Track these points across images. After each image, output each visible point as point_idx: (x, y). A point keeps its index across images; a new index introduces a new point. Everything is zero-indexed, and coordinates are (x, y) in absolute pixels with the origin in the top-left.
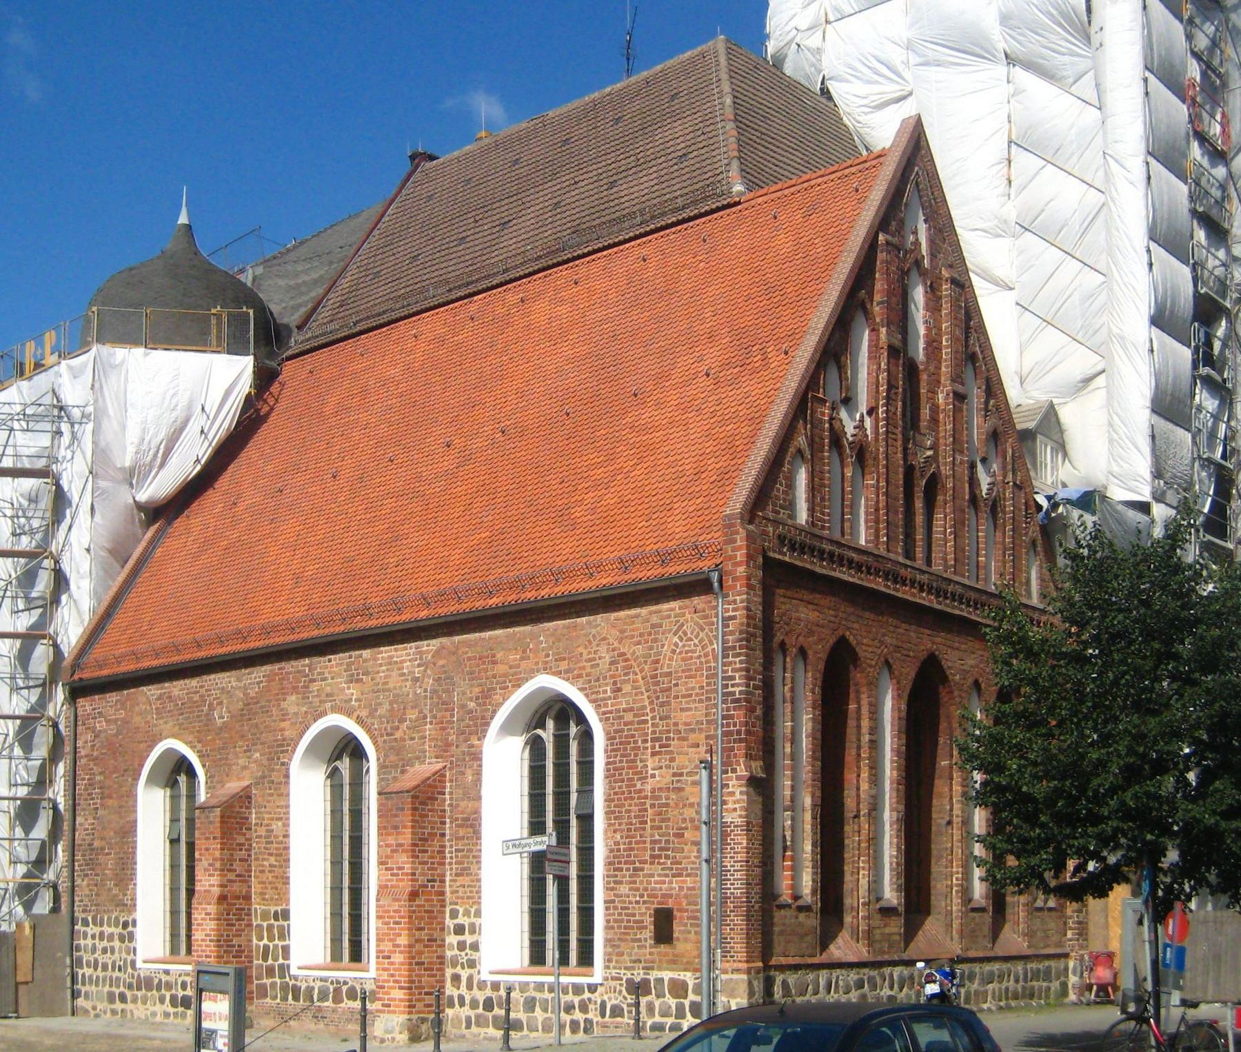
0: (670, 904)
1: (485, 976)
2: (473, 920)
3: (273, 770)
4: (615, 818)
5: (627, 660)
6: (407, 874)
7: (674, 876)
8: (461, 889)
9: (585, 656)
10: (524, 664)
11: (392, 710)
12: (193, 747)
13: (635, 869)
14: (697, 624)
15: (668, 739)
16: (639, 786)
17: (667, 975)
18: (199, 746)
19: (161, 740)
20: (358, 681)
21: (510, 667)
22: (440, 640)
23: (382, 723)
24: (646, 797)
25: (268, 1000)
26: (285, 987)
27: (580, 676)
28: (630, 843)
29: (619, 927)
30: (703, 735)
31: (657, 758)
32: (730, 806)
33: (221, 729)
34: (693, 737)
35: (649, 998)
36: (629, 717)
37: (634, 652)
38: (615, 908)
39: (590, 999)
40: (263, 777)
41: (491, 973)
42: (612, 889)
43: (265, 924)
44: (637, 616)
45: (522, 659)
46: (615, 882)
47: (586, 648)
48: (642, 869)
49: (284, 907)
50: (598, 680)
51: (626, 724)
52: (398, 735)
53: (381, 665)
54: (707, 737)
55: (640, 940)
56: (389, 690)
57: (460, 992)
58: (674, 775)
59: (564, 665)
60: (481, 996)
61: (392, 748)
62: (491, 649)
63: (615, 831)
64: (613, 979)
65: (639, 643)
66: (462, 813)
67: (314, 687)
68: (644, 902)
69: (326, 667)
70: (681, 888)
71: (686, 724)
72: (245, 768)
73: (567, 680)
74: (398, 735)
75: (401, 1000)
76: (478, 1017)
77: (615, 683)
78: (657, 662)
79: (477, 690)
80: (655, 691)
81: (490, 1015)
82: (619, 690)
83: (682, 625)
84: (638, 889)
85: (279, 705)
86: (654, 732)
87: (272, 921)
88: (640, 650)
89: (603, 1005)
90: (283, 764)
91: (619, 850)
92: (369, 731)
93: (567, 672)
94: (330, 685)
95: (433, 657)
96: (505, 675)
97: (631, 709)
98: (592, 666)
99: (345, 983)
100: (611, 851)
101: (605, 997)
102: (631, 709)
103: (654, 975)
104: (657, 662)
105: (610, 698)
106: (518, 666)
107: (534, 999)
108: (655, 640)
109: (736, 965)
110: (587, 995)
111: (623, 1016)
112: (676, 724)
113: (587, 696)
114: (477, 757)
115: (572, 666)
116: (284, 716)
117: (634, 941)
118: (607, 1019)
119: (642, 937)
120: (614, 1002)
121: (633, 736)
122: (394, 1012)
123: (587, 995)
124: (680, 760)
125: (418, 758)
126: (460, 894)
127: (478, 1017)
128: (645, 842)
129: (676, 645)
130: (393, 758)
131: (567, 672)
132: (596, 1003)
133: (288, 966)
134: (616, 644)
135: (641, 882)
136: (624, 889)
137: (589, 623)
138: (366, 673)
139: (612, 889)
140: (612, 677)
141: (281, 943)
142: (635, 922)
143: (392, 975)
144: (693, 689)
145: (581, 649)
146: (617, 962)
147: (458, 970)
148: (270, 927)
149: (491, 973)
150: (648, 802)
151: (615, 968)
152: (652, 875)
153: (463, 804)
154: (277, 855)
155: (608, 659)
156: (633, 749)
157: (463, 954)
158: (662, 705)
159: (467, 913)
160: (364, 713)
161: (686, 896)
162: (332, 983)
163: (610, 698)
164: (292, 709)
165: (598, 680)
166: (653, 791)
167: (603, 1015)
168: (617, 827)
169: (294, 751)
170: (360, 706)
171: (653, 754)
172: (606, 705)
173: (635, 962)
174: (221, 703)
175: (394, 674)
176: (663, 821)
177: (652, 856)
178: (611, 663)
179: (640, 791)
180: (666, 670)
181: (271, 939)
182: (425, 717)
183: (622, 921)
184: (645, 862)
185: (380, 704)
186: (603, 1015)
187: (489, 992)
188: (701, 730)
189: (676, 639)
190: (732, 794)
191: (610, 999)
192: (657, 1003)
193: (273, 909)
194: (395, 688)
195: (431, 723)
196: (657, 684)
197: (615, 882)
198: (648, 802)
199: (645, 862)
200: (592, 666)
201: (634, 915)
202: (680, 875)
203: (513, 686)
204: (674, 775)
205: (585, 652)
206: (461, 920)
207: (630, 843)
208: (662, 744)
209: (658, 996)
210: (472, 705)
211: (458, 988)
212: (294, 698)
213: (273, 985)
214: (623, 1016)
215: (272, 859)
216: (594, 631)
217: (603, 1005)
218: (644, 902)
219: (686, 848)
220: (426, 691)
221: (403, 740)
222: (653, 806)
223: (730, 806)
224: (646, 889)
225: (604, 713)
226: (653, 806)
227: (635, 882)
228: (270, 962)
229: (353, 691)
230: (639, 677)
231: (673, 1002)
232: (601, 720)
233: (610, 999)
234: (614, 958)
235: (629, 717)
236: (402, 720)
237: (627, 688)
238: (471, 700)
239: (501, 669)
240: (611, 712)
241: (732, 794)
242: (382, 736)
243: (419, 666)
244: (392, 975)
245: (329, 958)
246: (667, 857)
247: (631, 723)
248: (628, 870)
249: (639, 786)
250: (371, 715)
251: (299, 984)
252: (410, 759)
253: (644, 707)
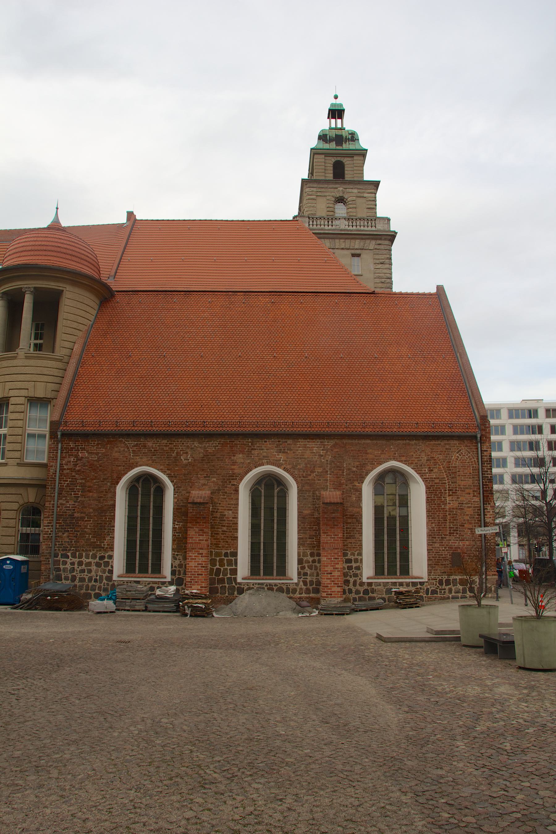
0: (459, 551)
1: (365, 580)
2: (356, 557)
3: (226, 487)
4: (432, 518)
5: (435, 460)
6: (340, 538)
7: (460, 540)
8: (349, 544)
9: (414, 456)
10: (383, 456)
11: (306, 467)
12: (164, 472)
13: (442, 538)
14: (467, 450)
15: (456, 490)
16: (443, 507)
17: (458, 577)
18: (169, 472)
19: (137, 467)
20: (284, 452)
21: (375, 456)
22: (336, 440)
23: (300, 472)
24: (446, 511)
25: (219, 594)
26: (232, 589)
27: (412, 463)
28: (439, 528)
29: (435, 560)
30: (472, 490)
31: (451, 497)
32: (488, 516)
33: (187, 465)
34: (467, 491)
35: (450, 586)
36: (437, 481)
37: (438, 457)
38: (433, 552)
39: (421, 588)
40: (219, 490)
41: (368, 578)
42: (431, 545)
43: (218, 559)
44: (440, 444)
45: (382, 454)
46: (433, 542)
47: (414, 453)
48: (446, 538)
49: (232, 550)
50: (421, 466)
51: (435, 483)
52: (310, 478)
53: (299, 447)
54: (473, 491)
55: (445, 564)
56: (305, 458)
57: (349, 587)
58: (459, 503)
59: (404, 458)
60: (362, 589)
61: (307, 483)
62: (364, 448)
63: (432, 523)
64: (432, 579)
65: (441, 454)
66: (350, 512)
67: (256, 452)
68: (447, 550)
69: (264, 444)
70: (464, 545)
71: (464, 486)
72: (204, 484)
73: (406, 464)
74: (310, 478)
75: (338, 592)
76: (360, 598)
77: (430, 468)
78: (450, 462)
79: (357, 463)
80: (449, 473)
81: (367, 597)
82: (432, 470)
83: (460, 450)
84: (443, 545)
85: (230, 458)
86: (449, 487)
87: (223, 557)
88: (441, 457)
89: (428, 589)
90: (234, 485)
91: (434, 530)
92: (292, 475)
93: (405, 461)
94: (266, 452)
95: (331, 447)
96: (373, 459)
97: (438, 478)
98: (418, 460)
99: (276, 585)
100: (430, 530)
101: (429, 587)
102: (438, 478)
103: (452, 578)
104: (450, 462)
105: (427, 473)
106: (380, 456)
107: (367, 590)
108: (449, 454)
109: (493, 573)
110: (419, 586)
111: (437, 594)
112: (459, 485)
113: (416, 471)
114: (360, 491)
115: (408, 459)
116: (234, 463)
117: (442, 565)
118: (429, 595)
119: (446, 563)
120: (432, 588)
121: (439, 488)
122: (334, 597)
123: (419, 586)
124: (461, 498)
125: (323, 488)
126: (349, 546)
127: (360, 598)
128: (446, 528)
129: (458, 457)
130: (307, 487)
131: (405, 461)
132: (424, 589)
133: (235, 579)
134: (429, 453)
135: (445, 543)
136: (437, 545)
137: (416, 444)
138: (291, 450)
139: (431, 545)
140: (428, 465)
141: (229, 568)
142: (442, 557)
143: (333, 581)
144: (467, 473)
145: (412, 453)
146: (434, 573)
147: (348, 578)
148: (221, 561)
149: (368, 578)
150: (448, 513)
151: (433, 575)
152: (450, 540)
153: (350, 509)
154: (227, 526)
155: (426, 458)
156: (440, 493)
157: (351, 571)
158: (453, 478)
159: (353, 554)
160: (288, 467)
161: (466, 548)
162: (267, 585)
163: (427, 473)
164: (239, 461)
165: (421, 466)
166: (450, 509)
167: (427, 594)
168: (433, 521)
169: (241, 480)
170: (286, 463)
171: (449, 495)
172: (426, 476)
173: (443, 573)
174: (187, 453)
175: (308, 452)
176: (455, 520)
177: (450, 533)
178: (427, 460)
179: (444, 509)
180: (453, 465)
181: (222, 564)
182: (327, 472)
183: (436, 557)
184: (447, 535)
185: (299, 464)
186: (427, 594)
187: (366, 587)
188: (471, 488)
189: (457, 455)
190: (489, 512)
191: (431, 587)
192: (453, 588)
193: (224, 552)
194: (308, 458)
195: (331, 474)
196: (450, 470)
197: (433, 542)
198: (448, 513)
199: (447, 535)
200: (418, 460)
201: (442, 555)
202: (463, 540)
203: (377, 464)
204: (459, 503)
205: (414, 455)
206: (349, 557)
207: (439, 528)
208: (453, 492)
209: (454, 586)
210: (354, 469)
211: (348, 586)
212: (241, 455)
213: (223, 588)
214: (437, 594)
215: (225, 529)
216: (418, 447)
217: (428, 589)
218: (447, 550)
219: (466, 530)
220: (327, 461)
221: (312, 480)
222: (449, 514)
223: (488, 516)
224: (448, 545)
225: (425, 478)
226: (449, 514)
227: (442, 543)
228: (221, 576)
229: (282, 457)
230: (441, 466)
231: (461, 587)
232: (423, 481)
233: (431, 587)
234: (433, 572)
235: (437, 481)
236: (312, 472)
237: (436, 470)
238: (354, 467)
239: (370, 456)
240: (428, 478)
241: (489, 512)
242: (300, 477)
243: (323, 450)
244: (333, 581)
245: (250, 575)
246: (456, 533)
247: (439, 483)
248: (439, 538)
249: (443, 507)
250: (293, 468)
251: (242, 587)
252: (318, 489)
253: (445, 478)
